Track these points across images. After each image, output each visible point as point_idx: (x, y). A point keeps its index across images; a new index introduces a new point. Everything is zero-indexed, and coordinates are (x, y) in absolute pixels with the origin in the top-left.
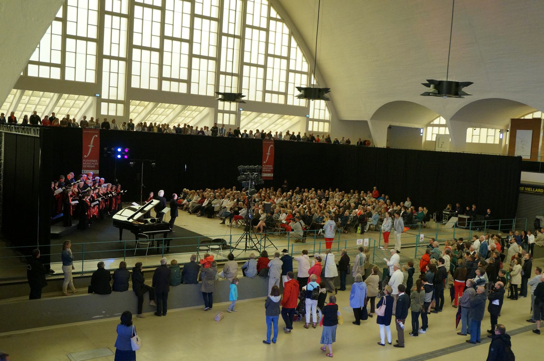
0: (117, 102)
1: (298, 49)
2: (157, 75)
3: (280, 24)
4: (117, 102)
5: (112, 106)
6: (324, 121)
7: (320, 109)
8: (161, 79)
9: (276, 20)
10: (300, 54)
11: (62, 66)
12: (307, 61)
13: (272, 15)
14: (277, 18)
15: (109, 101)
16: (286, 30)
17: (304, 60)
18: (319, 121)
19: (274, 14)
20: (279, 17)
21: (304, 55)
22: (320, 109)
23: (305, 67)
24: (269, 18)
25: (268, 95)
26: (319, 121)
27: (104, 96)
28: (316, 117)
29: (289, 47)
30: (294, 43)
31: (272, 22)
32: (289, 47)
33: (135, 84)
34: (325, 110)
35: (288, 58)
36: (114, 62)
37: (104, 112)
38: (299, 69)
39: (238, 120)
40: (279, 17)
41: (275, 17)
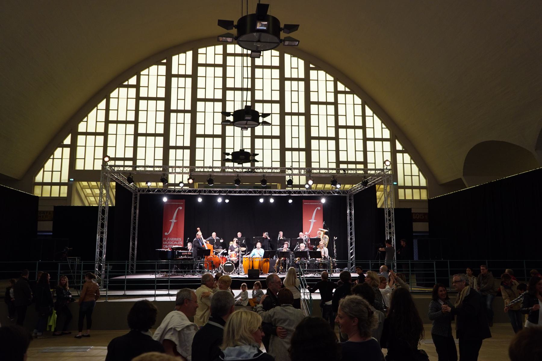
1: (375, 116)
3: (350, 97)
6: (420, 188)
10: (378, 121)
12: (387, 128)
14: (346, 90)
16: (358, 100)
17: (384, 126)
18: (412, 188)
19: (341, 87)
21: (382, 122)
22: (412, 176)
23: (387, 134)
24: (336, 92)
25: (342, 166)
28: (408, 184)
29: (364, 116)
30: (369, 112)
31: (341, 97)
32: (364, 116)
34: (419, 176)
35: (364, 127)
36: (180, 151)
40: (347, 90)
41: (344, 90)
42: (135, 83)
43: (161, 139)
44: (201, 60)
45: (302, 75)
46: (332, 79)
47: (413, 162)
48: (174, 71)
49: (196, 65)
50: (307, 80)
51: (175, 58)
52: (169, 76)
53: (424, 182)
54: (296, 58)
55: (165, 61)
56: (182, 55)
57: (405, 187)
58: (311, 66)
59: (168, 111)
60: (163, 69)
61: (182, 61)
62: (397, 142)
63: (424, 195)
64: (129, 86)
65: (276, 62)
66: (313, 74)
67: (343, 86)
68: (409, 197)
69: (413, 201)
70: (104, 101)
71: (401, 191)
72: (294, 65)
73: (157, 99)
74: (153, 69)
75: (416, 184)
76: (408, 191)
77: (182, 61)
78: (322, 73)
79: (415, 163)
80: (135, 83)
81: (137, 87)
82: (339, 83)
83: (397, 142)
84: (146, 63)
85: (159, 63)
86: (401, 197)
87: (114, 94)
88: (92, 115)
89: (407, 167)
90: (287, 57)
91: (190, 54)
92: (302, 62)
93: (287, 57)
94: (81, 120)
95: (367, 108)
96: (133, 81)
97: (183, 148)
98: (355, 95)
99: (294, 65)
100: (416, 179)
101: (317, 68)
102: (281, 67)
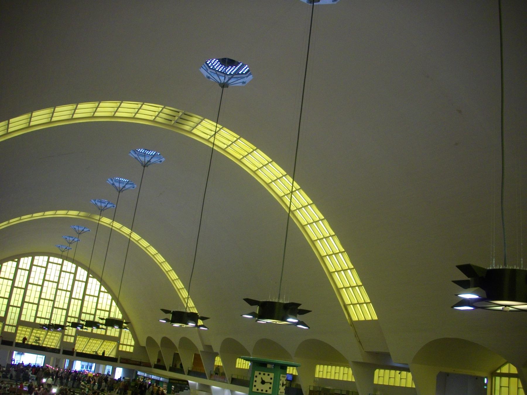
0: (12, 326)
2: (34, 315)
3: (106, 294)
4: (12, 326)
5: (10, 327)
6: (130, 346)
7: (128, 339)
8: (36, 317)
9: (104, 292)
12: (122, 313)
15: (9, 325)
16: (110, 297)
17: (120, 312)
18: (127, 345)
19: (103, 289)
20: (107, 291)
21: (119, 310)
26: (127, 345)
27: (7, 323)
28: (125, 343)
30: (114, 303)
33: (23, 318)
34: (131, 340)
36: (15, 308)
37: (6, 330)
39: (75, 340)
40: (106, 291)
41: (104, 291)
43: (7, 300)
44: (35, 263)
45: (85, 280)
46: (99, 284)
47: (130, 332)
48: (20, 266)
49: (32, 265)
50: (86, 282)
51: (22, 259)
52: (17, 268)
53: (133, 343)
54: (84, 270)
55: (16, 260)
56: (26, 258)
57: (123, 344)
58: (91, 275)
59: (13, 287)
60: (15, 264)
61: (25, 262)
63: (131, 349)
65: (73, 271)
66: (90, 279)
67: (104, 289)
68: (124, 349)
69: (126, 352)
71: (121, 346)
72: (82, 274)
73: (8, 279)
74: (10, 263)
75: (129, 344)
76: (124, 347)
77: (25, 262)
78: (95, 280)
79: (131, 333)
82: (102, 287)
84: (7, 260)
85: (13, 260)
86: (120, 349)
89: (127, 335)
90: (79, 268)
91: (30, 258)
92: (86, 273)
93: (79, 268)
95: (113, 302)
97: (17, 307)
98: (109, 294)
99: (82, 274)
100: (129, 341)
101: (93, 277)
102: (75, 274)
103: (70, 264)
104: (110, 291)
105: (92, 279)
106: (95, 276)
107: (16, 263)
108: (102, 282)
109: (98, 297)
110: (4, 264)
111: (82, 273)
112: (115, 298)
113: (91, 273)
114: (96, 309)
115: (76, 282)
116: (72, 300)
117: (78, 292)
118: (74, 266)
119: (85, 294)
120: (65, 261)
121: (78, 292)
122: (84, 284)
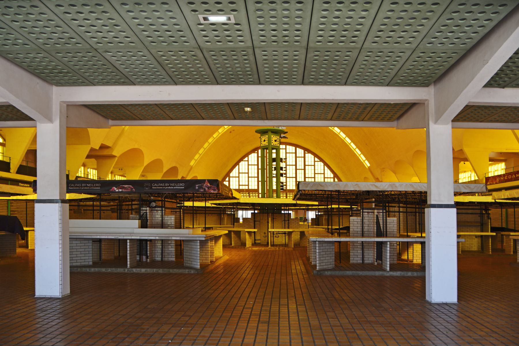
1: (328, 170)
3: (320, 163)
9: (318, 161)
10: (329, 171)
11: (248, 185)
13: (315, 160)
16: (322, 164)
17: (331, 173)
19: (316, 159)
23: (332, 176)
24: (315, 161)
30: (326, 168)
35: (324, 174)
38: (329, 177)
40: (319, 160)
41: (317, 160)
42: (247, 160)
45: (303, 156)
46: (313, 156)
50: (304, 157)
55: (256, 152)
58: (306, 152)
60: (256, 154)
62: (336, 179)
64: (245, 161)
70: (238, 166)
72: (300, 152)
74: (253, 154)
78: (310, 154)
80: (247, 160)
81: (248, 161)
82: (315, 158)
83: (336, 179)
87: (240, 164)
88: (234, 170)
90: (298, 149)
92: (303, 151)
93: (298, 149)
94: (231, 172)
95: (325, 166)
96: (246, 159)
99: (300, 152)
101: (308, 153)
102: (296, 153)
103: (291, 147)
104: (321, 160)
105: (307, 154)
106: (309, 152)
107: (256, 154)
108: (315, 155)
109: (314, 165)
110: (249, 156)
111: (300, 152)
112: (326, 164)
113: (306, 150)
114: (315, 174)
115: (297, 158)
116: (298, 171)
117: (300, 165)
118: (294, 148)
119: (305, 165)
120: (287, 146)
121: (300, 165)
122: (303, 158)
